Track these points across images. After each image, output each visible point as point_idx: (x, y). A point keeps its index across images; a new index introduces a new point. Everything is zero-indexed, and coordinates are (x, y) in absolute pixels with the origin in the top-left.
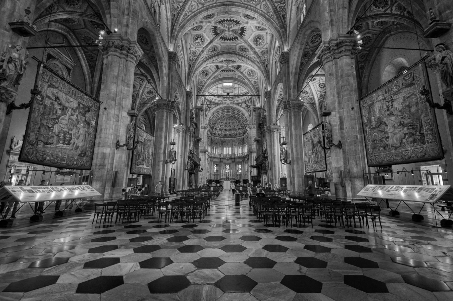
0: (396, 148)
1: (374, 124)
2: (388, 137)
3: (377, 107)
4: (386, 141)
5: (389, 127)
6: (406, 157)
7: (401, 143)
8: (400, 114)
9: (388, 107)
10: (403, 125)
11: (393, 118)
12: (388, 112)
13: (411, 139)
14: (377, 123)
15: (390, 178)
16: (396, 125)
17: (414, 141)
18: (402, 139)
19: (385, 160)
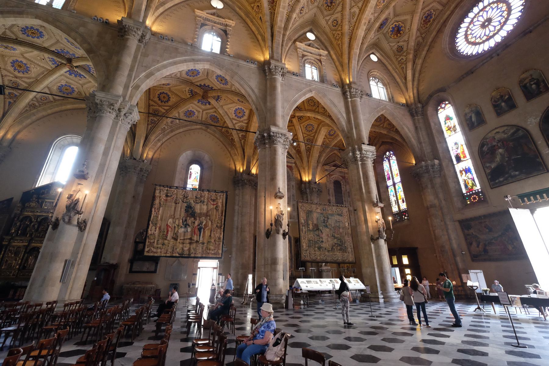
0: (328, 251)
1: (311, 227)
2: (322, 242)
3: (315, 215)
4: (320, 244)
5: (324, 234)
6: (335, 259)
7: (332, 248)
8: (333, 229)
9: (324, 220)
10: (335, 238)
11: (328, 230)
12: (324, 224)
13: (339, 248)
14: (314, 228)
15: (153, 269)
16: (329, 235)
17: (340, 249)
18: (333, 246)
19: (319, 258)
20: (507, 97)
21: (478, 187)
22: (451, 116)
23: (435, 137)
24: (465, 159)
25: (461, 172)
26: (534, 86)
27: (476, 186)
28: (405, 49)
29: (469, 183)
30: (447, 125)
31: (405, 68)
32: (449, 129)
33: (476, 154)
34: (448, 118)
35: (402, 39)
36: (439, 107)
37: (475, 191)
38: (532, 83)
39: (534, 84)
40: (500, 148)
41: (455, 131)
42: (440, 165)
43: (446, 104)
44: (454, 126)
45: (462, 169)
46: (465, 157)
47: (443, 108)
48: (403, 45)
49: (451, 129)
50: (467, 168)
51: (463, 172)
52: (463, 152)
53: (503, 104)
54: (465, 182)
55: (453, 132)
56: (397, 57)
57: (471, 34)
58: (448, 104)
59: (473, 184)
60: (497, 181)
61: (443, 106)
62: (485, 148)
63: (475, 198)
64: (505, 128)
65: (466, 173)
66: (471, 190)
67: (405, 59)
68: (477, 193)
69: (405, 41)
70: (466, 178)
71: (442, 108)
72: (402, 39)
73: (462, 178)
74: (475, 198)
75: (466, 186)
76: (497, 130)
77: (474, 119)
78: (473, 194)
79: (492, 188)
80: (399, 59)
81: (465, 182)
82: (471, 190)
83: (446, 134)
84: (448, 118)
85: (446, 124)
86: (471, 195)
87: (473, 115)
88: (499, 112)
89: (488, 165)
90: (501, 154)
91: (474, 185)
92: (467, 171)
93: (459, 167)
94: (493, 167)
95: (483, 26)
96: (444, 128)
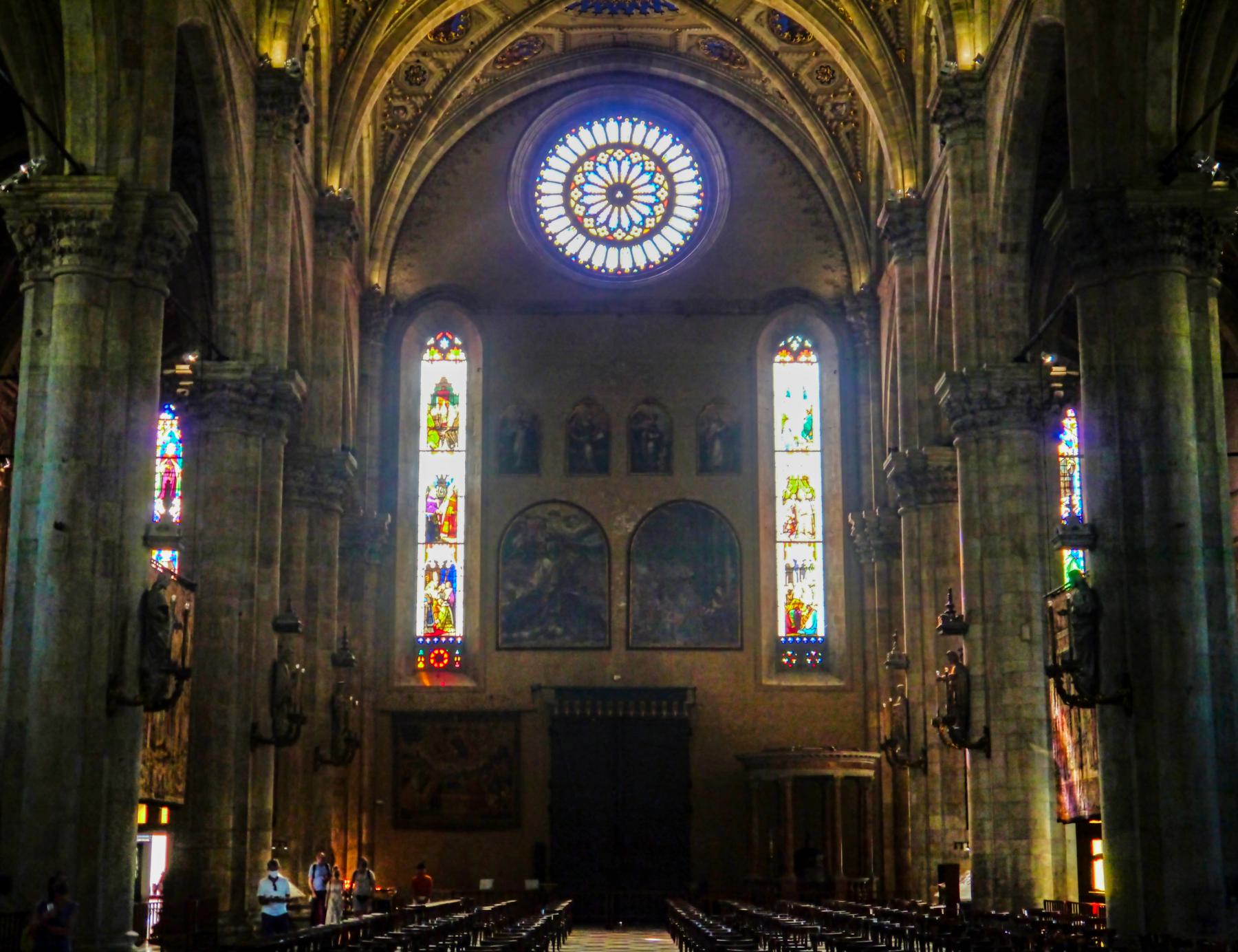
20: (600, 436)
21: (457, 631)
22: (455, 392)
23: (401, 438)
24: (451, 540)
25: (429, 571)
26: (651, 445)
27: (454, 627)
28: (429, 88)
29: (438, 612)
30: (435, 411)
31: (394, 143)
32: (438, 427)
33: (493, 543)
34: (444, 393)
35: (440, 56)
36: (431, 341)
37: (448, 638)
38: (651, 436)
39: (653, 440)
40: (547, 555)
41: (451, 443)
42: (393, 526)
43: (452, 345)
44: (454, 429)
45: (433, 566)
46: (452, 533)
47: (440, 351)
48: (431, 73)
49: (443, 433)
50: (448, 566)
51: (435, 575)
52: (452, 519)
53: (588, 448)
54: (431, 604)
55: (446, 447)
56: (396, 91)
57: (580, 187)
58: (458, 347)
59: (448, 617)
60: (515, 635)
61: (444, 344)
62: (517, 541)
63: (439, 658)
64: (574, 512)
65: (441, 581)
66: (438, 632)
67: (409, 117)
68: (451, 645)
69: (441, 63)
70: (435, 595)
71: (436, 346)
72: (440, 56)
73: (426, 591)
74: (439, 658)
75: (429, 618)
76: (556, 508)
77: (518, 446)
78: (439, 645)
79: (498, 649)
80: (397, 103)
81: (431, 604)
82: (438, 632)
83: (425, 440)
84: (444, 393)
85: (433, 405)
86: (432, 647)
87: (521, 434)
88: (575, 466)
89: (510, 586)
90: (545, 571)
91: (449, 620)
92: (447, 575)
93: (430, 555)
94: (518, 595)
95: (611, 191)
96: (424, 421)
